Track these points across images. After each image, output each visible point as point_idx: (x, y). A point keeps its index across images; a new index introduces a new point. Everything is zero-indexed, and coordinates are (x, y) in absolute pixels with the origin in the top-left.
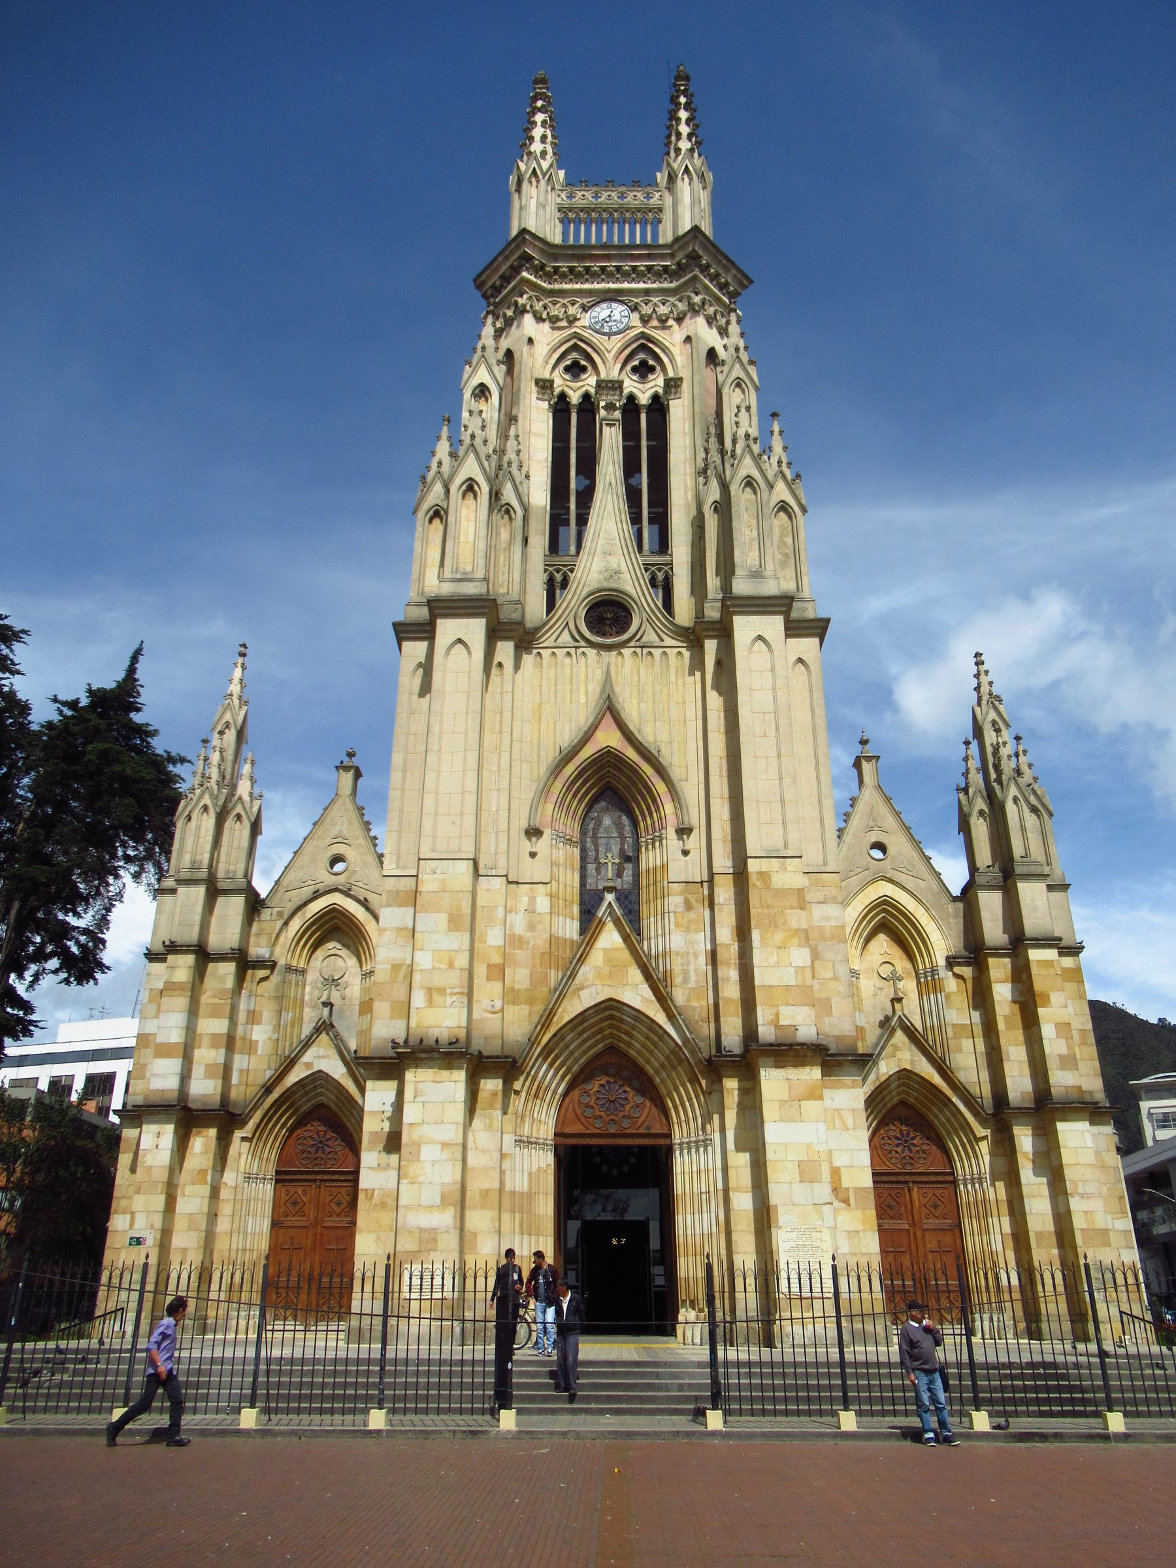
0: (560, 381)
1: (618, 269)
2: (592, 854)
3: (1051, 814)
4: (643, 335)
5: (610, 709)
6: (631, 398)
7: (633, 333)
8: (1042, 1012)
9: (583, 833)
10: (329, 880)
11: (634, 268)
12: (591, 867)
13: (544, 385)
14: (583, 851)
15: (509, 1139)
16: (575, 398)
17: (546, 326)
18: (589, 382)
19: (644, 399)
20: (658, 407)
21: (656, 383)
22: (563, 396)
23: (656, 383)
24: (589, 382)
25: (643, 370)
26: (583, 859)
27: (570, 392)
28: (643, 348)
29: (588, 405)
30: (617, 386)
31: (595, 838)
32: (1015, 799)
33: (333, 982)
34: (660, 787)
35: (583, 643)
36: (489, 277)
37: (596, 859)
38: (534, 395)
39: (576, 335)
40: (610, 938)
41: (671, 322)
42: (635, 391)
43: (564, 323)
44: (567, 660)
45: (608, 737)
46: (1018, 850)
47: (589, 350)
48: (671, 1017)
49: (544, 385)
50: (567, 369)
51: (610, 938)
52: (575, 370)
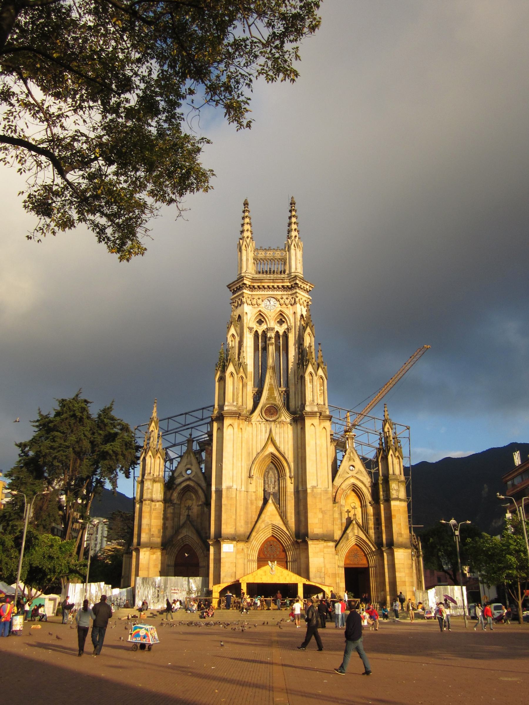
0: (256, 327)
1: (273, 286)
2: (266, 482)
3: (402, 459)
4: (281, 311)
5: (271, 439)
6: (277, 332)
7: (278, 310)
8: (393, 520)
9: (264, 476)
10: (186, 477)
11: (278, 286)
12: (266, 486)
13: (250, 329)
14: (264, 481)
15: (246, 561)
16: (260, 332)
17: (250, 307)
18: (264, 327)
19: (281, 333)
20: (286, 336)
21: (285, 326)
22: (256, 331)
23: (285, 326)
24: (264, 327)
25: (281, 322)
26: (264, 483)
27: (258, 331)
28: (281, 314)
29: (264, 333)
30: (273, 329)
31: (268, 478)
32: (391, 455)
33: (189, 508)
34: (285, 464)
35: (264, 420)
36: (232, 286)
37: (268, 483)
38: (248, 333)
39: (260, 311)
40: (271, 507)
41: (289, 306)
42: (278, 330)
43: (256, 306)
44: (259, 426)
45: (271, 449)
46: (391, 472)
47: (264, 316)
48: (288, 529)
49: (250, 329)
50: (258, 322)
51: (271, 507)
52: (260, 322)
